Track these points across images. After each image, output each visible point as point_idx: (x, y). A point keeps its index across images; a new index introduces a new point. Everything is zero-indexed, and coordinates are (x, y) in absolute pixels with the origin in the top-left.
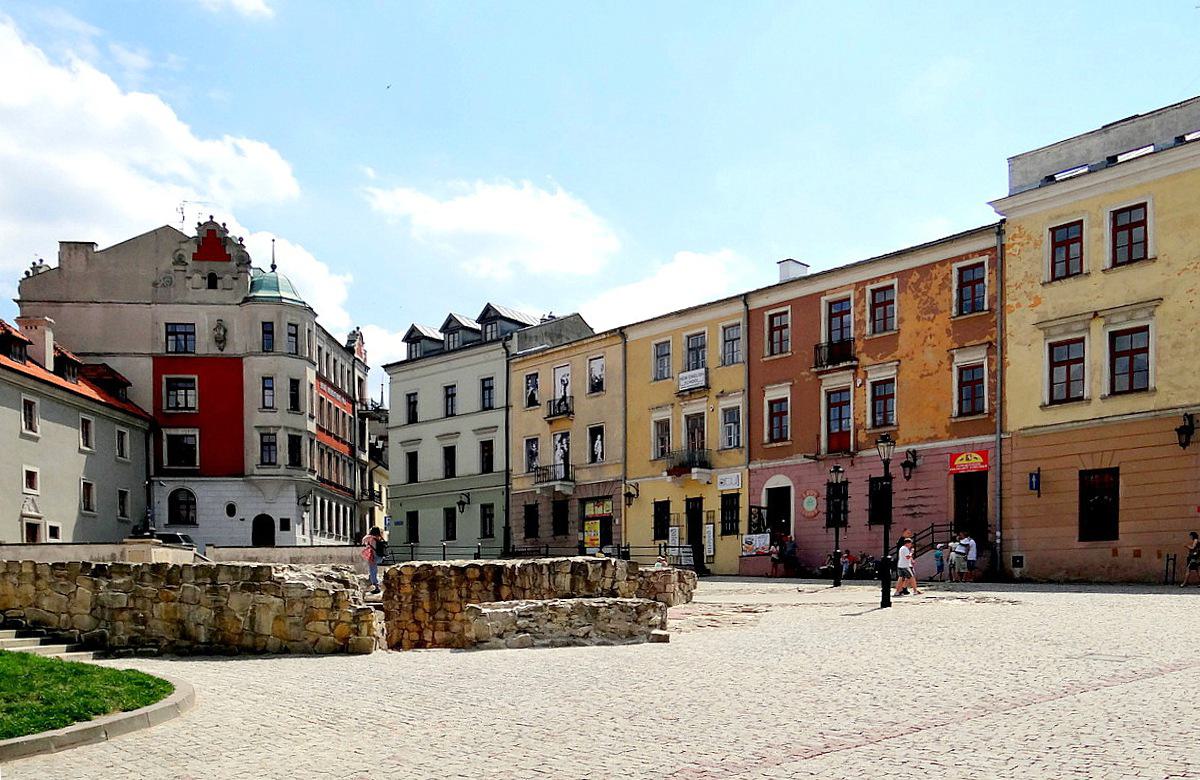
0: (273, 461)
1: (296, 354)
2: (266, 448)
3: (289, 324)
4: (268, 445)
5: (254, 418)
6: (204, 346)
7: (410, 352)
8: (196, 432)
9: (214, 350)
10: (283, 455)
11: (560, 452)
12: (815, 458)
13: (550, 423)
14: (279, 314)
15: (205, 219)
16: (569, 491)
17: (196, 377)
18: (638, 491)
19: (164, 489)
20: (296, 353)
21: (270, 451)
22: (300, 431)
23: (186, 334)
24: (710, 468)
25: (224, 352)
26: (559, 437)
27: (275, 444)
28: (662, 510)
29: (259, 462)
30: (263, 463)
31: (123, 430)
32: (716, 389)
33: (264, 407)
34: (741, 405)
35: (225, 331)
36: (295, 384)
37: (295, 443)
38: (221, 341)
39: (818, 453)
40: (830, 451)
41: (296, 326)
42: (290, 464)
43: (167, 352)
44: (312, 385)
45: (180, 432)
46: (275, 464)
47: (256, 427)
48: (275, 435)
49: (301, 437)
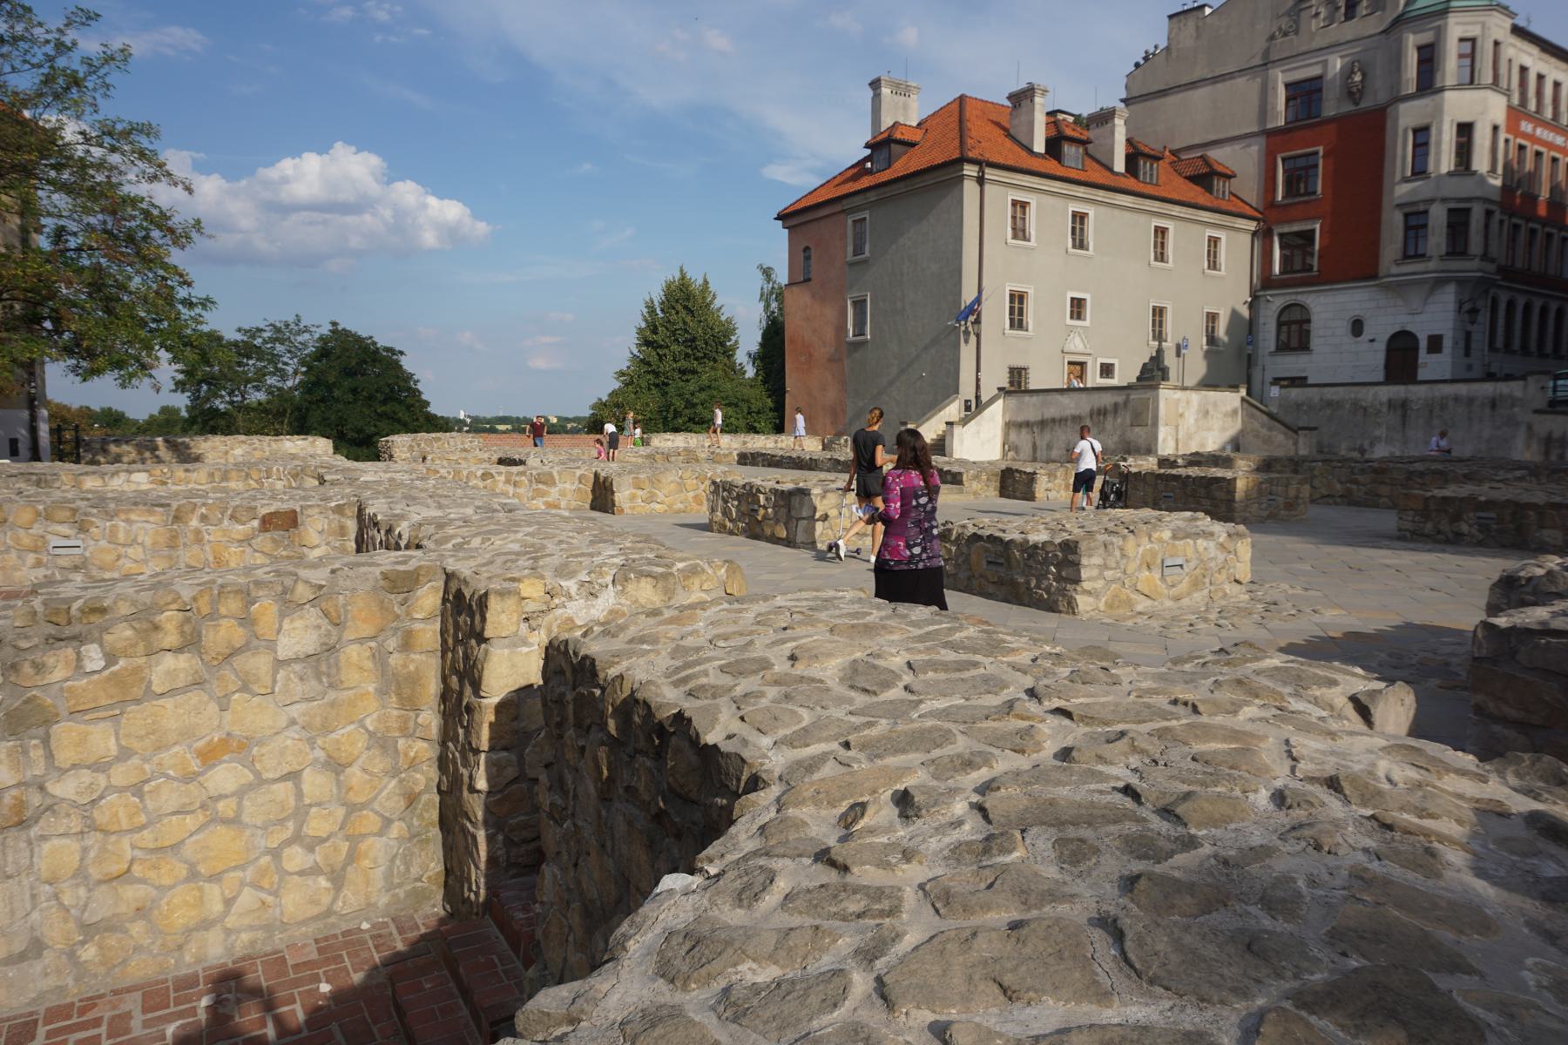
0: (1420, 251)
1: (1472, 82)
2: (1412, 233)
3: (1462, 40)
5: (1402, 191)
6: (1331, 107)
9: (1348, 107)
10: (1436, 240)
14: (1440, 33)
17: (1321, 149)
19: (1276, 302)
20: (1472, 82)
22: (1469, 200)
25: (1363, 105)
27: (1425, 226)
29: (1399, 255)
30: (1406, 257)
31: (1216, 233)
36: (1465, 130)
38: (1352, 94)
41: (1473, 40)
42: (1448, 254)
44: (1495, 128)
45: (1296, 228)
46: (1423, 255)
47: (1399, 206)
48: (1426, 212)
49: (1468, 211)
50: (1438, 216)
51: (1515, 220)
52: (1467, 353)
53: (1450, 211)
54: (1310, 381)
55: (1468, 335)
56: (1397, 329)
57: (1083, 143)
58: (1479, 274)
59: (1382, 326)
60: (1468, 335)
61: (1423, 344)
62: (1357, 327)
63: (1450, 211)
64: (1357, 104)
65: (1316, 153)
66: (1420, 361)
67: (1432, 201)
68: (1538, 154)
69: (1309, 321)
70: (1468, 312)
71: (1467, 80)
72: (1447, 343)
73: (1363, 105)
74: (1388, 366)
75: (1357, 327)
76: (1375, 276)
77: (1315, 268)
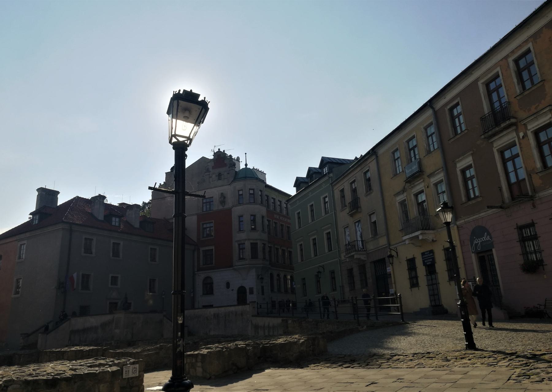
3: (250, 189)
4: (241, 249)
5: (238, 237)
7: (297, 191)
8: (213, 247)
9: (221, 207)
10: (248, 253)
11: (359, 233)
12: (501, 207)
13: (352, 216)
15: (216, 150)
16: (363, 257)
17: (213, 221)
18: (397, 253)
21: (243, 252)
23: (210, 202)
24: (433, 229)
25: (225, 207)
26: (357, 224)
28: (411, 263)
32: (428, 171)
33: (240, 230)
34: (443, 178)
35: (224, 198)
37: (254, 246)
39: (503, 202)
40: (513, 198)
41: (253, 190)
43: (203, 212)
44: (263, 217)
45: (207, 248)
46: (244, 259)
48: (244, 244)
49: (257, 243)
50: (248, 245)
51: (276, 246)
52: (263, 294)
53: (251, 243)
54: (214, 306)
55: (263, 287)
56: (240, 286)
57: (119, 217)
58: (262, 265)
59: (235, 285)
60: (263, 287)
61: (248, 291)
62: (228, 285)
63: (251, 243)
64: (223, 207)
65: (212, 222)
66: (247, 297)
67: (246, 240)
68: (282, 225)
69: (213, 283)
70: (260, 278)
71: (253, 202)
72: (255, 290)
73: (225, 207)
74: (238, 300)
75: (228, 285)
76: (231, 266)
77: (214, 264)
